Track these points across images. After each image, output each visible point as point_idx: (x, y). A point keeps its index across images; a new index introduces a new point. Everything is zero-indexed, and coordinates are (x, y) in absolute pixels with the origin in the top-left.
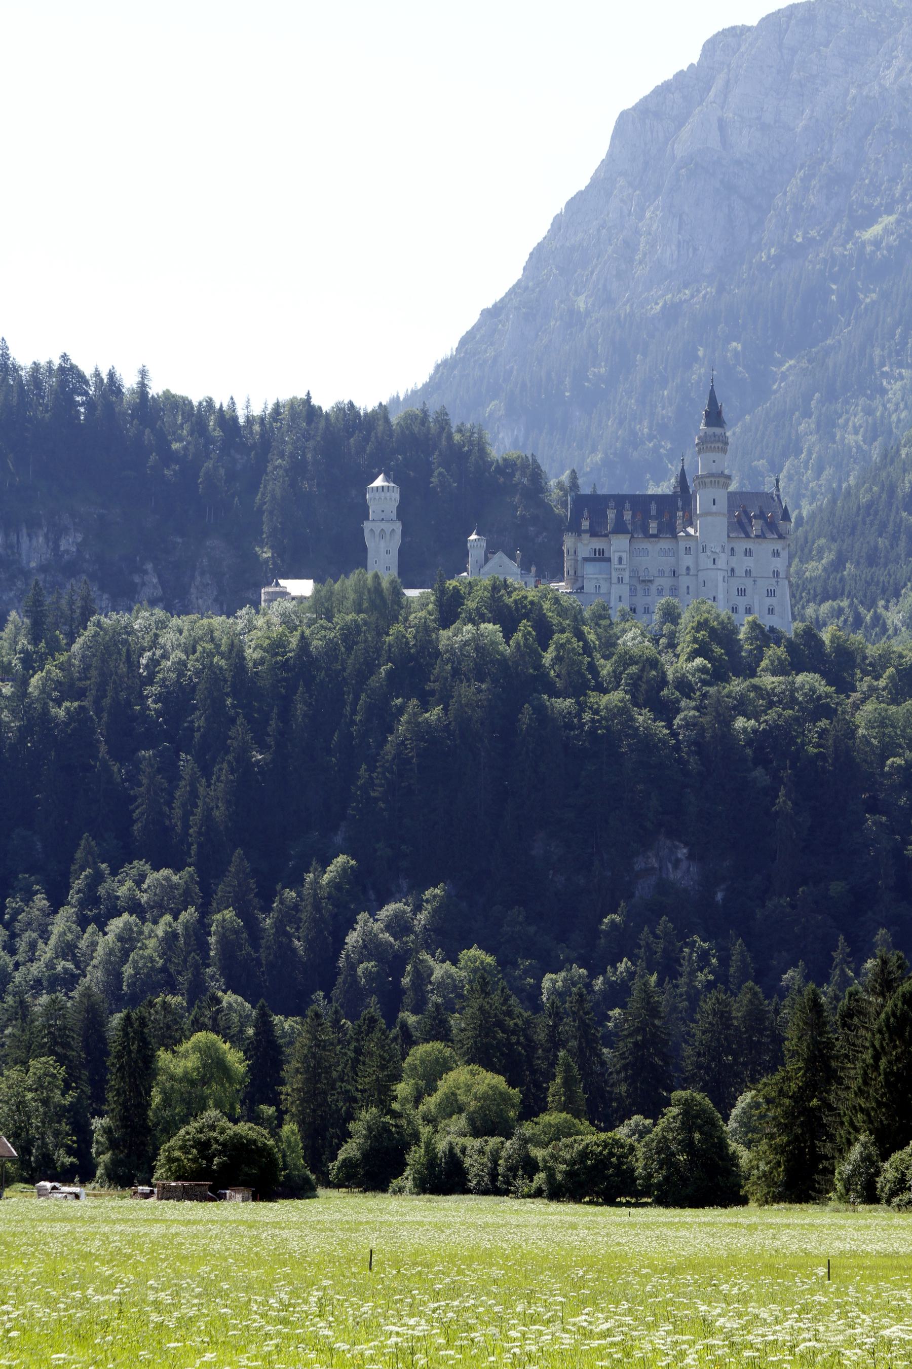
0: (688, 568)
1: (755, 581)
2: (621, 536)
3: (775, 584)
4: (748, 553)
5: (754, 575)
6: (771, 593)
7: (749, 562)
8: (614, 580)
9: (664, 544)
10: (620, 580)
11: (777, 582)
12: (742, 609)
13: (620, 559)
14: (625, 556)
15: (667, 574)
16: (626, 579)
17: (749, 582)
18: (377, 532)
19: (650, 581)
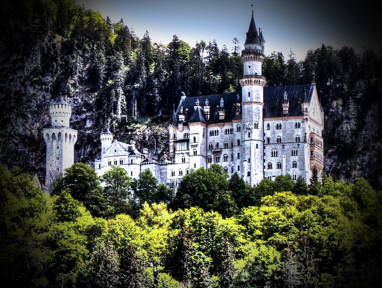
0: (239, 141)
1: (283, 146)
2: (194, 124)
3: (297, 146)
4: (279, 127)
5: (282, 142)
6: (294, 153)
7: (280, 134)
8: (191, 153)
9: (227, 127)
10: (195, 153)
11: (298, 145)
12: (274, 166)
13: (195, 138)
14: (196, 136)
15: (229, 146)
16: (198, 153)
17: (279, 147)
18: (51, 136)
19: (218, 152)
